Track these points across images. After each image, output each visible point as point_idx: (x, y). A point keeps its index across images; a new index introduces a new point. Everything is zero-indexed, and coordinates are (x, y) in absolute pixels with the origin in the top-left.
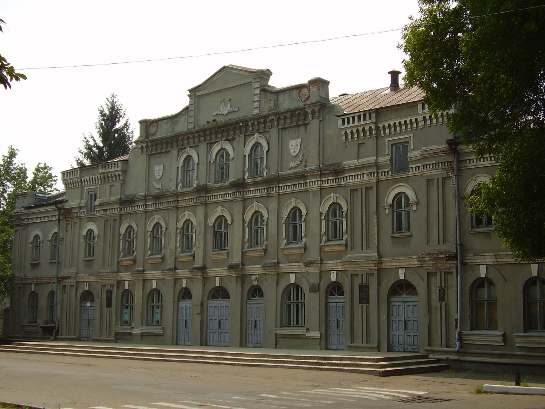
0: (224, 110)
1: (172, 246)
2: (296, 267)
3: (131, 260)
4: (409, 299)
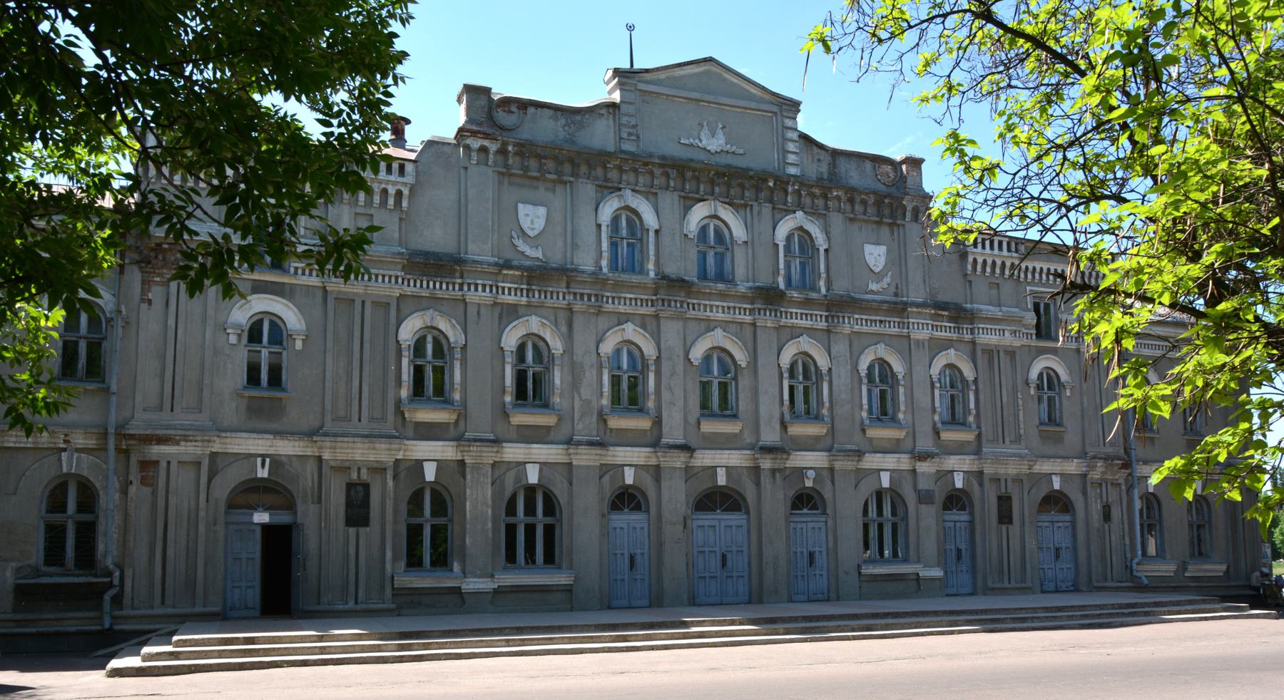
0: (714, 143)
2: (890, 461)
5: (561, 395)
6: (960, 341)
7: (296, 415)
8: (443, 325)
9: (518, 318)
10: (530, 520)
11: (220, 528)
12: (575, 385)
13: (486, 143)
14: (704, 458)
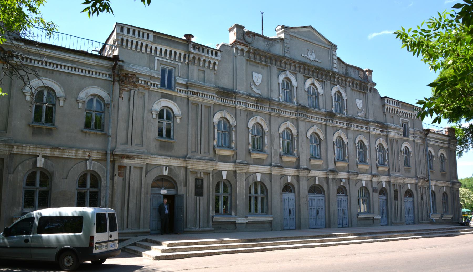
0: (312, 57)
5: (267, 148)
7: (179, 148)
8: (228, 117)
9: (253, 116)
11: (149, 196)
12: (271, 144)
13: (244, 47)
14: (313, 173)
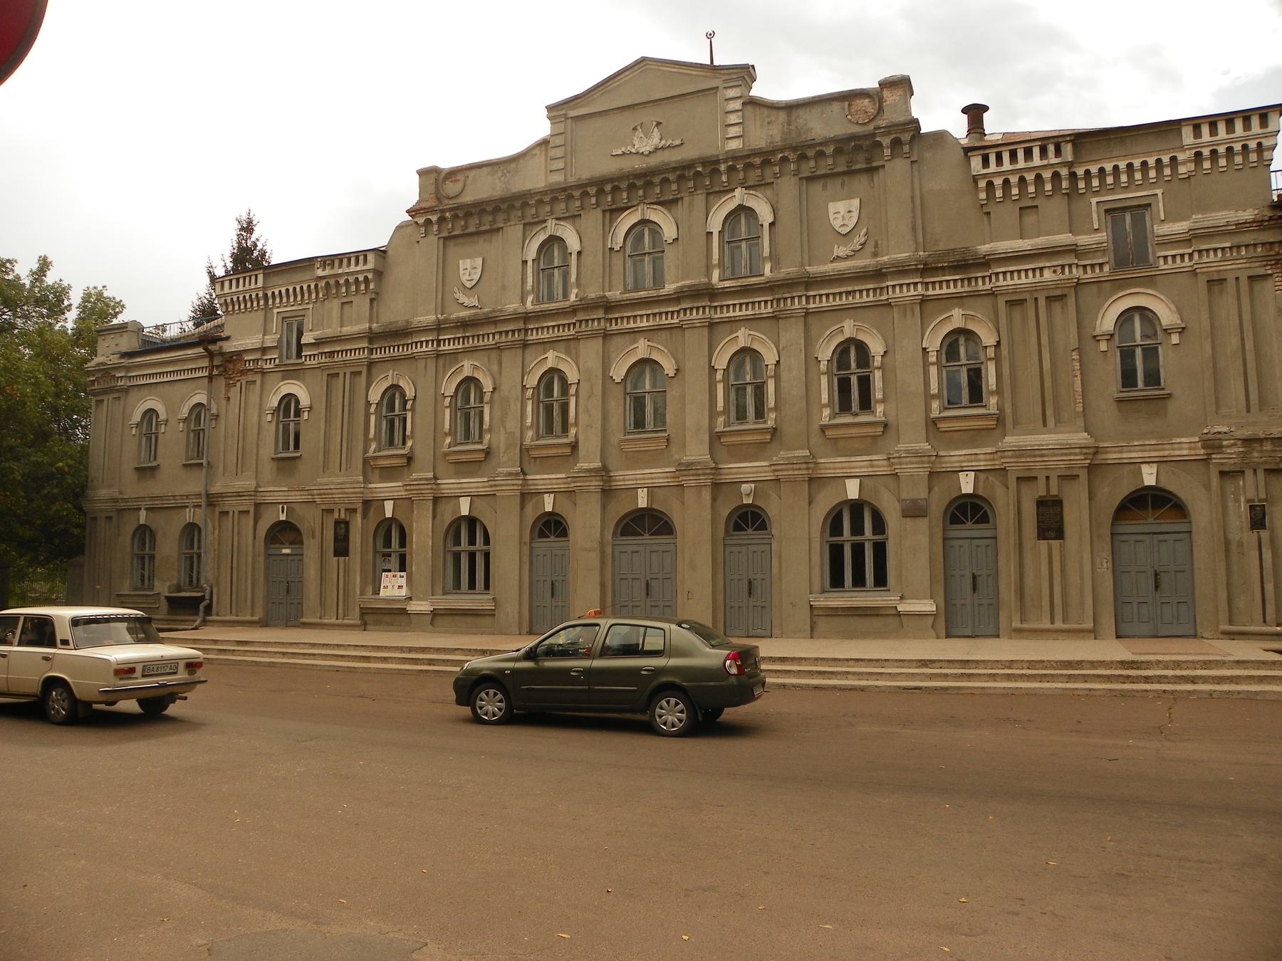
0: (646, 143)
1: (512, 425)
3: (402, 456)
4: (1164, 528)
6: (975, 295)
10: (472, 548)
